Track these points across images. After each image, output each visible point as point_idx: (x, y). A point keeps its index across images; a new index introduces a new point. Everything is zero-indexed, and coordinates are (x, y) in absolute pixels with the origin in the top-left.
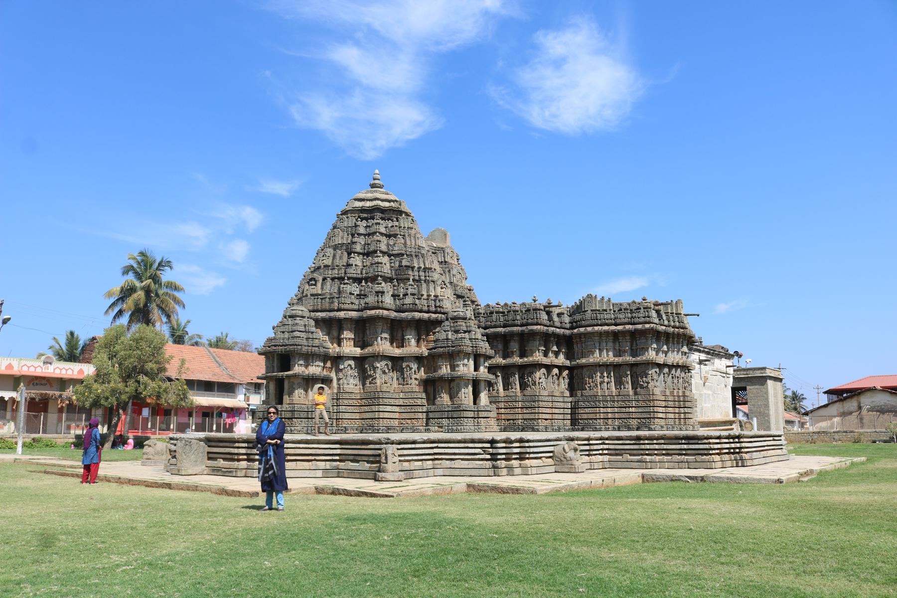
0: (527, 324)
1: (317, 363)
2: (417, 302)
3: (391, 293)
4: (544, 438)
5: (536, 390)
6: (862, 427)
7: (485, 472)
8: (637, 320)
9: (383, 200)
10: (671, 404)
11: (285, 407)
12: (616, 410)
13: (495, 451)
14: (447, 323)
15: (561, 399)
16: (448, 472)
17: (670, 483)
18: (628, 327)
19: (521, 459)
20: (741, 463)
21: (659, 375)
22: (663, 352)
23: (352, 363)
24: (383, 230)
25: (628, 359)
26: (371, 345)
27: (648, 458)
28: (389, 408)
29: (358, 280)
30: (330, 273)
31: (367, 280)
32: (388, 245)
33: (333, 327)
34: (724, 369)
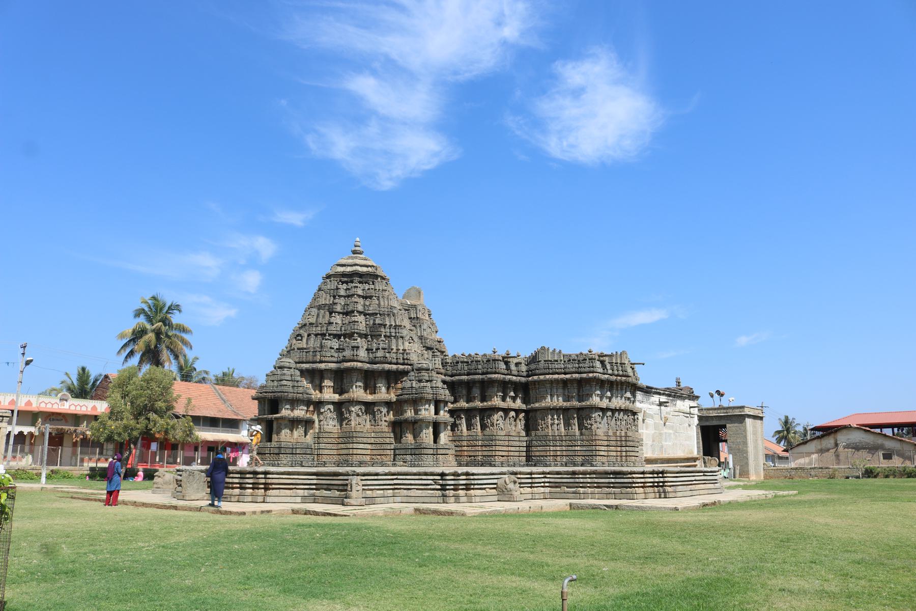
0: (487, 373)
1: (302, 407)
2: (387, 355)
3: (365, 347)
4: (488, 472)
5: (494, 430)
6: (838, 463)
7: (436, 500)
8: (582, 370)
9: (361, 266)
10: (613, 443)
11: (274, 444)
12: (564, 448)
13: (444, 482)
14: (412, 373)
15: (517, 439)
16: (405, 499)
17: (592, 511)
18: (575, 376)
19: (468, 489)
20: (664, 495)
21: (602, 418)
22: (607, 397)
23: (331, 407)
24: (360, 292)
25: (575, 403)
26: (347, 392)
27: (581, 490)
28: (361, 446)
29: (337, 336)
30: (314, 330)
31: (345, 336)
32: (364, 305)
33: (315, 376)
34: (688, 410)
